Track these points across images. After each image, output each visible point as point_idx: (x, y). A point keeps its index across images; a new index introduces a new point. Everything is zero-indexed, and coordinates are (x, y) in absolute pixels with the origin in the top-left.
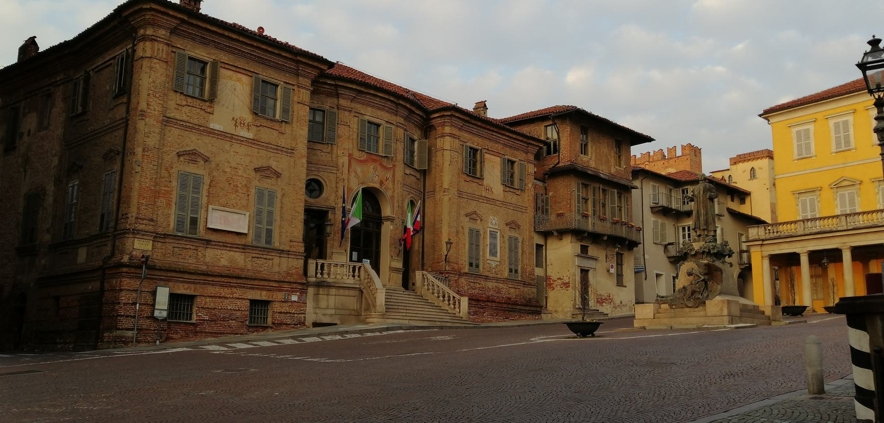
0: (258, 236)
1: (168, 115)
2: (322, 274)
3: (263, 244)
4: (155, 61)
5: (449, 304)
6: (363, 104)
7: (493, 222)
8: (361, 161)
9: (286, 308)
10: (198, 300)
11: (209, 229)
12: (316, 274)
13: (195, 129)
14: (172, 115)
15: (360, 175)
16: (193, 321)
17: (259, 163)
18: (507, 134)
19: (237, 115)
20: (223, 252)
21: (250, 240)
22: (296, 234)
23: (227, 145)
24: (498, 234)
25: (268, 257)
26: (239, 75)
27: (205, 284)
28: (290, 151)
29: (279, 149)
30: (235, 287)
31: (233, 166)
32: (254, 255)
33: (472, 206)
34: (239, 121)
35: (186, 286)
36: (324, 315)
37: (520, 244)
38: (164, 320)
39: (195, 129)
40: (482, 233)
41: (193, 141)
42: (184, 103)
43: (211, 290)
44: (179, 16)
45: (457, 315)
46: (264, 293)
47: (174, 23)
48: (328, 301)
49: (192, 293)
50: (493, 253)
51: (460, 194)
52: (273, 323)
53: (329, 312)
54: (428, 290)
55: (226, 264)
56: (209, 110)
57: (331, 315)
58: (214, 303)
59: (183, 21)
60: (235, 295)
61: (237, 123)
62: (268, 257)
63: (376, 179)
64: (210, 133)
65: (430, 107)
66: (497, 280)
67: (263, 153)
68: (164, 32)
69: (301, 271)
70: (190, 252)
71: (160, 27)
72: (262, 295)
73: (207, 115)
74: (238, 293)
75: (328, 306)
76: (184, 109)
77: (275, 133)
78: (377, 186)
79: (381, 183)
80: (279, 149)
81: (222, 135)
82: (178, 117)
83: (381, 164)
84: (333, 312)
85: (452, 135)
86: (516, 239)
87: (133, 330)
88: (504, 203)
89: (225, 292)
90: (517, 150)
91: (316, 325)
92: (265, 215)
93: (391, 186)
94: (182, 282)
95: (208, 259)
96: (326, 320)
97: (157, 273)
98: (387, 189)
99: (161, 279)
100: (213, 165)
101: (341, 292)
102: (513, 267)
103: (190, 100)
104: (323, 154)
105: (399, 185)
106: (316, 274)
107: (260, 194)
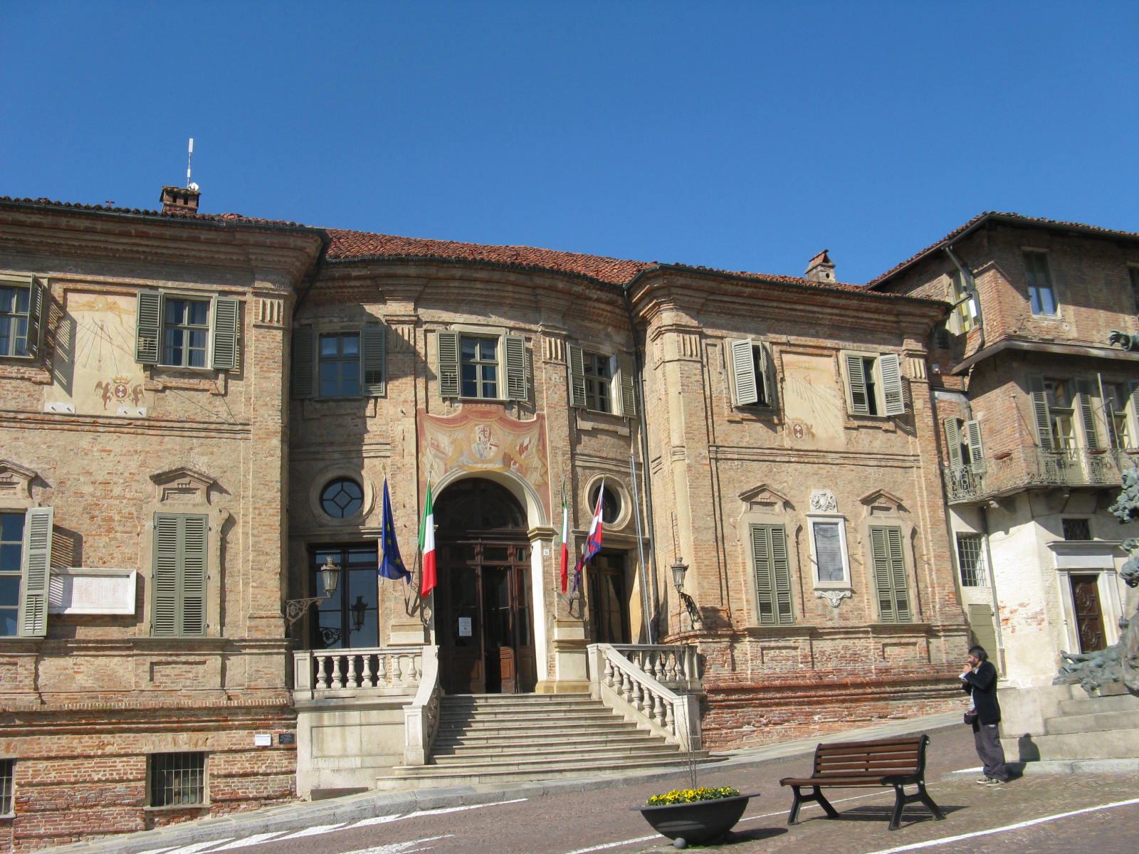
0: (163, 619)
2: (329, 681)
3: (178, 633)
5: (652, 716)
7: (816, 497)
8: (448, 421)
9: (241, 763)
12: (315, 681)
15: (449, 450)
16: (12, 814)
17: (165, 466)
18: (832, 300)
19: (108, 376)
21: (142, 631)
23: (85, 440)
24: (841, 527)
25: (191, 659)
26: (111, 298)
28: (238, 429)
31: (100, 479)
32: (155, 659)
33: (754, 476)
34: (112, 388)
36: (338, 771)
37: (907, 542)
40: (791, 530)
45: (670, 741)
46: (183, 737)
48: (344, 739)
50: (827, 568)
51: (717, 453)
52: (214, 801)
53: (346, 763)
54: (611, 685)
55: (89, 683)
57: (353, 770)
58: (58, 771)
60: (109, 750)
62: (191, 659)
64: (43, 422)
65: (624, 279)
66: (849, 632)
67: (172, 442)
69: (280, 682)
72: (183, 743)
73: (37, 387)
74: (115, 743)
75: (345, 750)
77: (203, 398)
78: (496, 467)
79: (507, 459)
80: (209, 429)
83: (503, 420)
84: (357, 762)
85: (679, 329)
86: (894, 531)
88: (849, 456)
91: (320, 794)
92: (180, 570)
93: (536, 462)
96: (340, 783)
98: (523, 470)
101: (374, 715)
102: (893, 598)
106: (315, 681)
107: (165, 527)
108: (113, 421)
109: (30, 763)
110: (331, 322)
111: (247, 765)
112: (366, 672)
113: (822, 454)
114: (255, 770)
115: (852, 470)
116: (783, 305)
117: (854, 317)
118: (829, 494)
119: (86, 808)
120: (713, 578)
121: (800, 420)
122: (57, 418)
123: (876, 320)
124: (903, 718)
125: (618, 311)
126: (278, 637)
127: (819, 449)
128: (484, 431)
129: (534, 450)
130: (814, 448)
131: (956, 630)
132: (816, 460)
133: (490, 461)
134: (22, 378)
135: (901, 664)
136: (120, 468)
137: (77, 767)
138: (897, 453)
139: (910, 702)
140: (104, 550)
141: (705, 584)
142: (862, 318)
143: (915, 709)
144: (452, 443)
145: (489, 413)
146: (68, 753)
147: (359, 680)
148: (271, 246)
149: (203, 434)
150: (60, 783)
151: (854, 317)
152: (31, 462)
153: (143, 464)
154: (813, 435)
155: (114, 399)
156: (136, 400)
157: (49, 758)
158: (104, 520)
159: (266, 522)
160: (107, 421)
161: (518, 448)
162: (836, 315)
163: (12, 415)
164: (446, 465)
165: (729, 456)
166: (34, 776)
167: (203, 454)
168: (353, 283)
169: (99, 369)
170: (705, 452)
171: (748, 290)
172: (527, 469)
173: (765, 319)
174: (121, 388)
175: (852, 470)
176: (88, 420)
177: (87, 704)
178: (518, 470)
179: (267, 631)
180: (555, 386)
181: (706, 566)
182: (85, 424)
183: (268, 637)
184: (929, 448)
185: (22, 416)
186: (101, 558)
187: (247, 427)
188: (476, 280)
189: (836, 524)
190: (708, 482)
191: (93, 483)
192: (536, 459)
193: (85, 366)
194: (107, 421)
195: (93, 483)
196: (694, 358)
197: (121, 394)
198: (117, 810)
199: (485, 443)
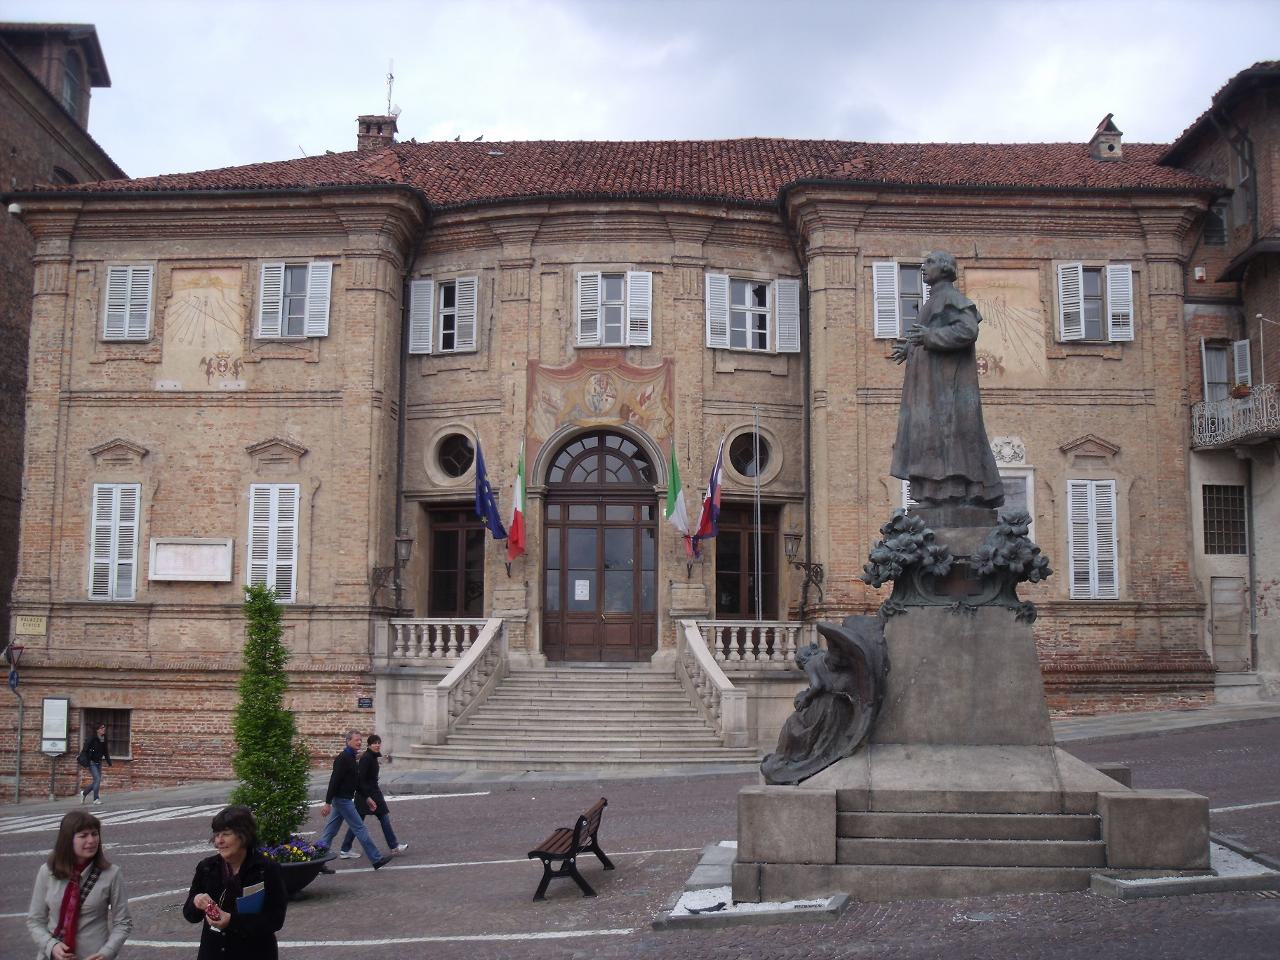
1: (74, 387)
4: (45, 298)
6: (565, 240)
10: (133, 717)
11: (157, 583)
13: (124, 400)
14: (83, 385)
16: (130, 758)
17: (260, 436)
19: (210, 352)
20: (185, 623)
22: (349, 568)
23: (190, 416)
26: (214, 274)
27: (144, 687)
28: (332, 397)
29: (304, 398)
30: (208, 689)
34: (214, 364)
35: (108, 692)
38: (62, 757)
39: (124, 400)
41: (127, 425)
42: (103, 357)
43: (157, 698)
44: (67, 206)
47: (68, 221)
49: (119, 705)
55: (192, 644)
56: (151, 358)
58: (165, 721)
59: (79, 212)
60: (207, 705)
61: (208, 367)
63: (608, 404)
64: (154, 400)
67: (269, 413)
68: (58, 243)
70: (120, 630)
71: (50, 235)
73: (150, 367)
76: (105, 368)
77: (299, 366)
79: (625, 412)
80: (304, 398)
81: (180, 399)
82: (94, 386)
83: (623, 368)
87: (12, 774)
89: (185, 699)
90: (1102, 232)
93: (660, 412)
94: (98, 686)
95: (153, 640)
97: (49, 674)
99: (60, 685)
100: (161, 459)
103: (115, 349)
104: (472, 376)
105: (689, 407)
108: (214, 396)
109: (142, 714)
110: (449, 271)
111: (328, 726)
112: (439, 642)
113: (1011, 392)
114: (336, 731)
115: (1052, 412)
116: (969, 212)
117: (1071, 217)
118: (1016, 441)
119: (189, 755)
120: (850, 544)
121: (985, 351)
122: (166, 395)
123: (1104, 218)
124: (1088, 714)
125: (777, 230)
126: (362, 604)
127: (1008, 386)
128: (600, 381)
129: (658, 400)
130: (1002, 386)
131: (1180, 610)
132: (1002, 401)
133: (606, 414)
134: (137, 359)
135: (1094, 649)
136: (222, 441)
137: (180, 719)
138: (1122, 387)
139: (1100, 697)
140: (206, 521)
141: (840, 551)
142: (1084, 218)
143: (1105, 704)
144: (564, 396)
145: (608, 361)
146: (173, 706)
147: (446, 649)
148: (359, 206)
149: (297, 404)
150: (167, 732)
151: (1071, 217)
152: (144, 439)
153: (242, 436)
154: (1002, 370)
155: (217, 373)
156: (236, 373)
157: (157, 710)
158: (206, 492)
159: (356, 489)
160: (209, 396)
161: (638, 398)
162: (1046, 217)
163: (127, 395)
164: (557, 420)
165: (884, 400)
166: (146, 726)
167: (297, 424)
168: (467, 229)
169: (204, 345)
170: (853, 398)
171: (918, 199)
172: (648, 421)
173: (946, 230)
174: (223, 363)
175: (1052, 412)
176: (192, 396)
177: (186, 664)
178: (637, 422)
179: (352, 598)
180: (688, 325)
181: (843, 529)
182: (189, 399)
183: (352, 604)
184: (1169, 379)
185: (136, 396)
186: (203, 528)
187: (339, 395)
188: (593, 214)
189: (1024, 478)
190: (852, 432)
191: (197, 456)
192: (661, 409)
193: (190, 343)
194: (209, 396)
195: (197, 456)
196: (846, 285)
197: (222, 369)
198: (213, 760)
199: (600, 395)
